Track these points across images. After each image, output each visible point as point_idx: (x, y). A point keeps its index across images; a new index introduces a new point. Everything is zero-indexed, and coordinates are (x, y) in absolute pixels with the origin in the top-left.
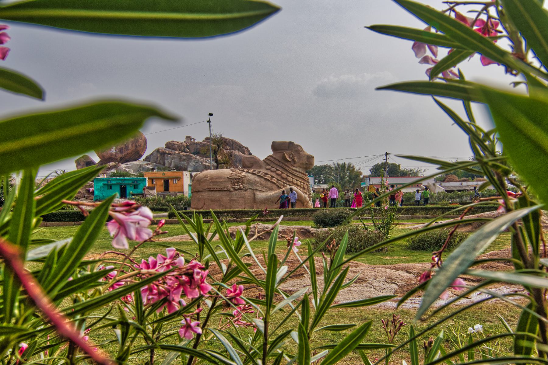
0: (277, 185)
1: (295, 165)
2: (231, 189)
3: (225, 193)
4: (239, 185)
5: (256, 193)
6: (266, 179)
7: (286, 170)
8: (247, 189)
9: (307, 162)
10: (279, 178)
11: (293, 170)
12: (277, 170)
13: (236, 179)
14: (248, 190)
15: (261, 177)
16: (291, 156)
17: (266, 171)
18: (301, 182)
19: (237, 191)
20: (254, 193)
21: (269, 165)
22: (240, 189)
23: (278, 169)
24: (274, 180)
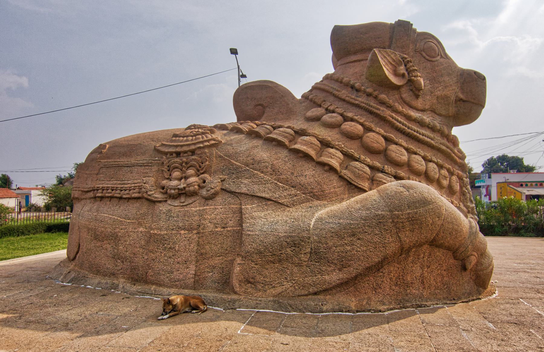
0: (341, 178)
1: (419, 103)
2: (158, 196)
3: (133, 209)
4: (186, 178)
5: (249, 207)
6: (297, 152)
7: (383, 120)
8: (215, 194)
9: (461, 96)
10: (353, 149)
11: (409, 118)
12: (346, 119)
13: (178, 154)
14: (219, 199)
15: (280, 144)
16: (402, 69)
17: (299, 124)
18: (441, 167)
19: (176, 203)
20: (241, 211)
21: (320, 106)
22: (182, 193)
23: (350, 115)
24: (332, 156)
